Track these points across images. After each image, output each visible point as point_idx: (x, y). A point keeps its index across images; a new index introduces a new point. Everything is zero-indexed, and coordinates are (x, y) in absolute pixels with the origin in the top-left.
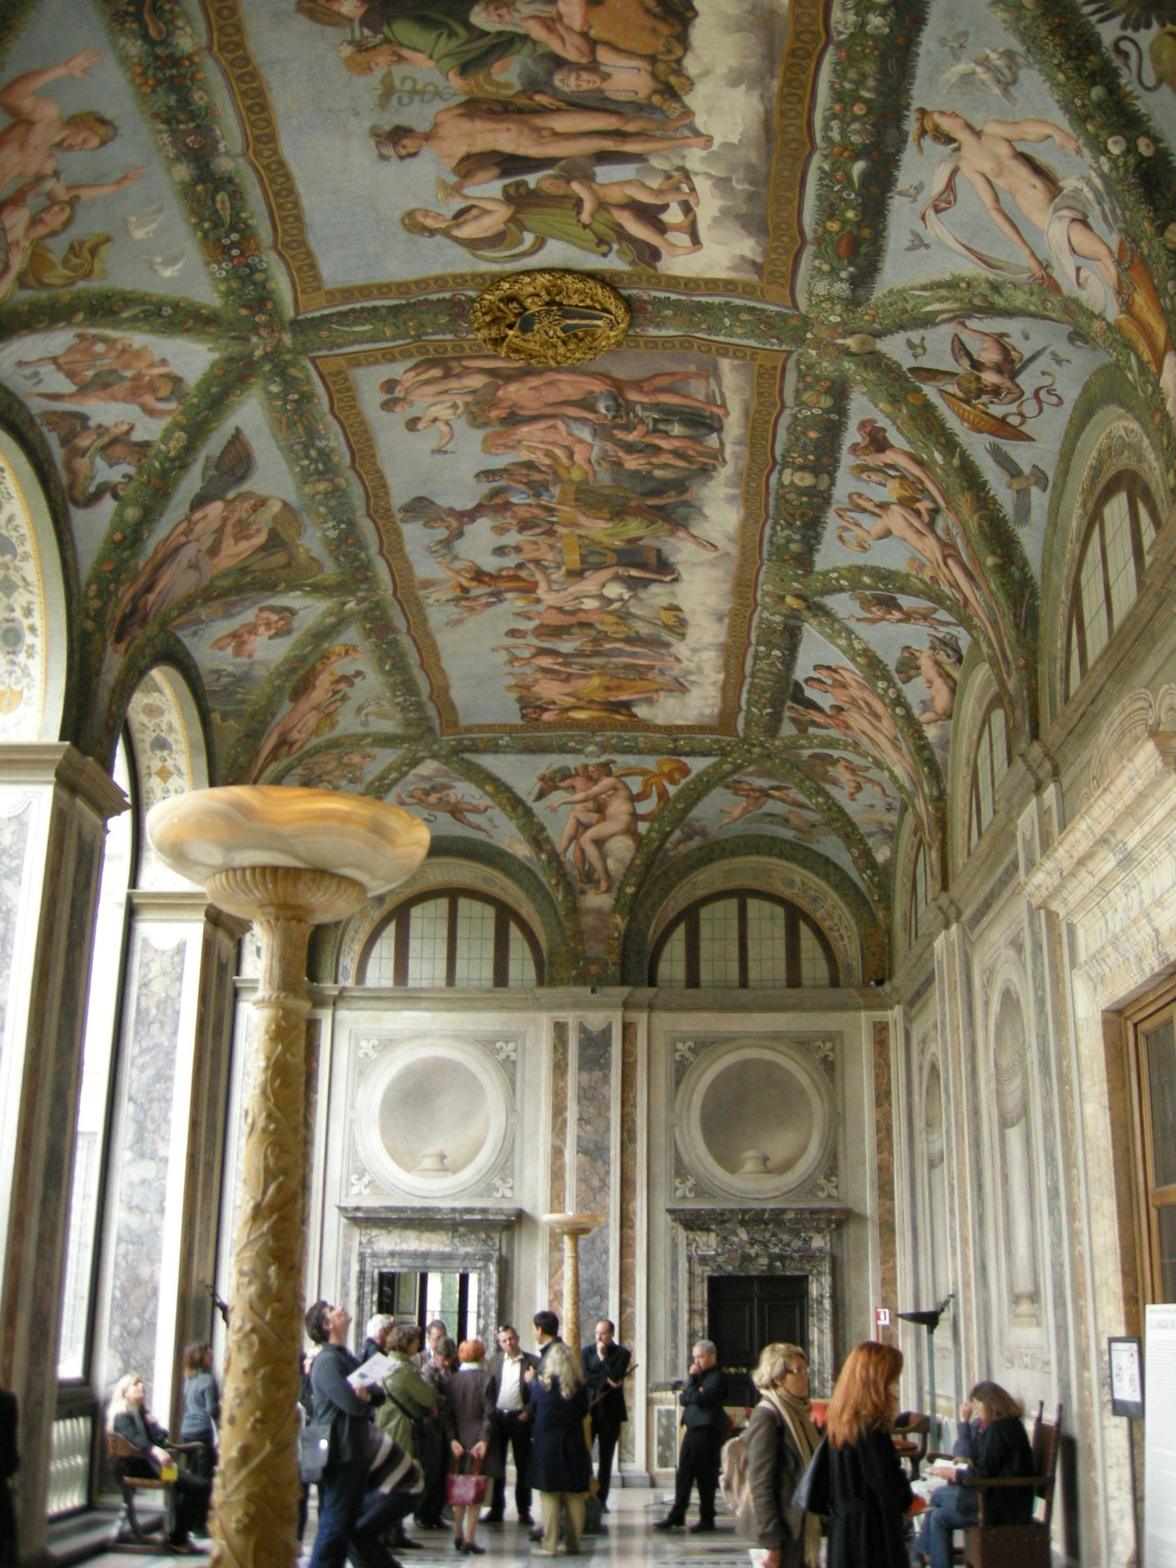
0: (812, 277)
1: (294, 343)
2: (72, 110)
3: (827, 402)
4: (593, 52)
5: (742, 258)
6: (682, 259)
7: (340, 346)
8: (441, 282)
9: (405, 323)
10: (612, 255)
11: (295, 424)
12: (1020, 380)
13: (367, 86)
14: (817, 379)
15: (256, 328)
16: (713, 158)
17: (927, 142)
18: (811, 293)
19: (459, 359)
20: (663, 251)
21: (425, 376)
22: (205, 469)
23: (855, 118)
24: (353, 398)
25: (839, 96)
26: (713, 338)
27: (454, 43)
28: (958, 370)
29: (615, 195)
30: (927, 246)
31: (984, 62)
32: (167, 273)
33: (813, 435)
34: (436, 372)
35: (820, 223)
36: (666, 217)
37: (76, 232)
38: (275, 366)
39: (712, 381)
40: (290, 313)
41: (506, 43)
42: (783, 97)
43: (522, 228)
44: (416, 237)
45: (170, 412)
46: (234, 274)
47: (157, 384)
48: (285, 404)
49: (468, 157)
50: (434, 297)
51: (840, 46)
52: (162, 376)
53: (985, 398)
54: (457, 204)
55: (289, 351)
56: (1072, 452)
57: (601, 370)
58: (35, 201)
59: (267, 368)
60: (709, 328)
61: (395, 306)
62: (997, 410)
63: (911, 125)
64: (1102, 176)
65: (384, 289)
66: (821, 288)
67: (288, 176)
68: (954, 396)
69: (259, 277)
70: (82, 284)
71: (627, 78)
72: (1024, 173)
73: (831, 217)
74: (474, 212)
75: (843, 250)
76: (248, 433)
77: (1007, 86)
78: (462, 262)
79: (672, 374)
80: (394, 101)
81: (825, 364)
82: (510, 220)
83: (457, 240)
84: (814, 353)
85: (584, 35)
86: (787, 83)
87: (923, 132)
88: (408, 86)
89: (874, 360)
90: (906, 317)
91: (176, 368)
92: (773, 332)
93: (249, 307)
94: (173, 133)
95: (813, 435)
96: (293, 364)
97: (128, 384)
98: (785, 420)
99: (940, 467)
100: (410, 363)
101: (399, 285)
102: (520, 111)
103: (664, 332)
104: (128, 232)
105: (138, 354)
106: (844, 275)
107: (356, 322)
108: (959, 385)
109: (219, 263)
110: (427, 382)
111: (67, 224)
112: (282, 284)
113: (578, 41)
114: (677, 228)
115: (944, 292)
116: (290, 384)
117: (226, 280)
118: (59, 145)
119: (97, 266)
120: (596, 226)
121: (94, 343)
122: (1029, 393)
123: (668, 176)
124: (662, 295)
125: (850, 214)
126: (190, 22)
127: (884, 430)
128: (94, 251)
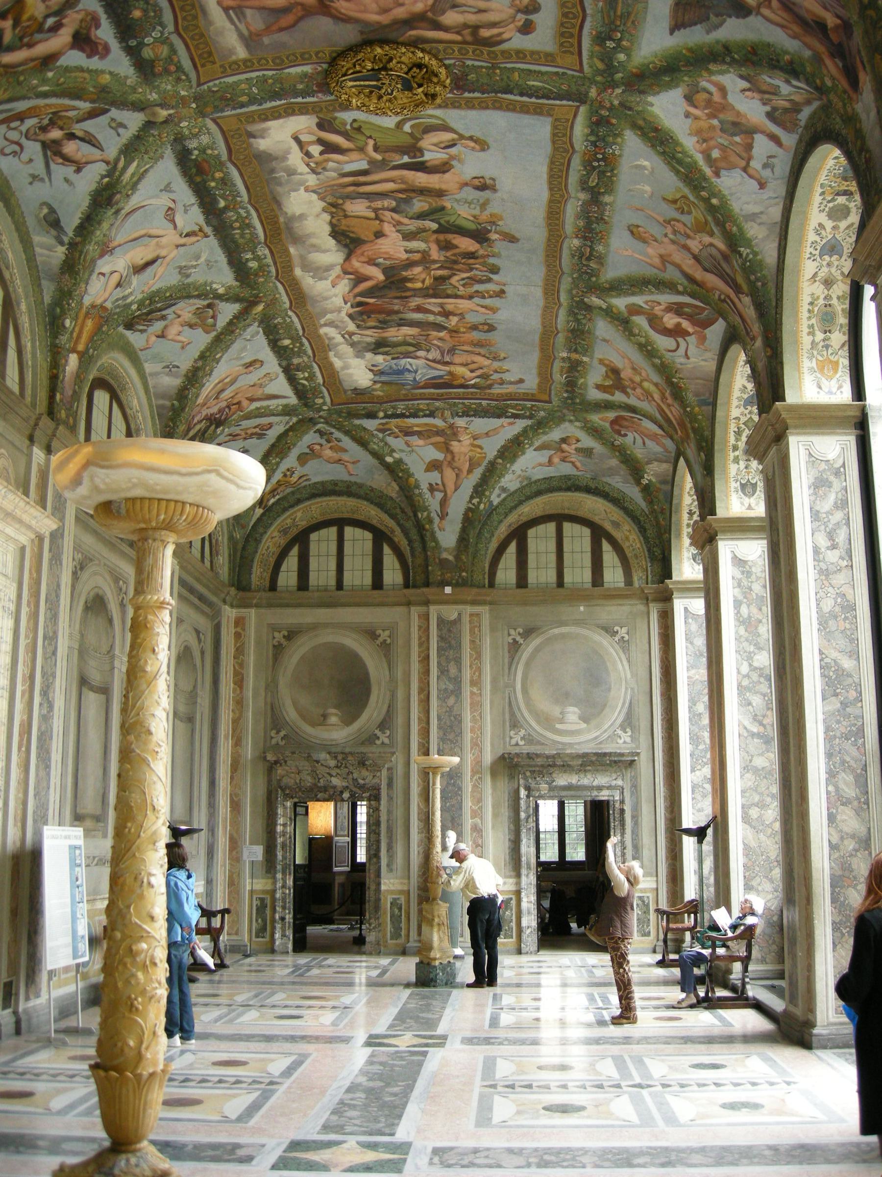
0: (214, 143)
1: (590, 87)
2: (642, 244)
3: (147, 53)
4: (377, 215)
5: (263, 138)
6: (302, 127)
7: (557, 73)
8: (470, 105)
9: (502, 79)
10: (349, 121)
11: (621, 17)
12: (38, 146)
13: (494, 208)
14: (167, 71)
15: (611, 108)
16: (302, 183)
17: (196, 228)
18: (209, 133)
19: (465, 42)
20: (316, 129)
21: (495, 31)
22: (717, 27)
23: (236, 221)
24: (562, 25)
25: (249, 226)
26: (260, 73)
27: (447, 218)
28: (78, 126)
29: (354, 155)
30: (161, 191)
31: (195, 267)
32: (646, 163)
33: (137, 14)
34: (485, 33)
35: (227, 174)
36: (320, 148)
37: (677, 215)
38: (612, 75)
39: (246, 32)
40: (583, 109)
41: (421, 216)
42: (276, 216)
43: (411, 135)
44: (482, 138)
45: (708, 81)
46: (608, 145)
47: (703, 104)
48: (621, 40)
49: (444, 172)
50: (477, 95)
51: (260, 243)
52: (696, 107)
53: (46, 122)
54: (453, 151)
55: (596, 83)
56: (18, 230)
57: (341, 25)
58: (682, 240)
59: (619, 76)
60: (266, 81)
61: (506, 93)
62: (30, 123)
63: (208, 230)
64: (131, 304)
65: (511, 107)
66: (205, 139)
67: (550, 183)
68: (67, 111)
69: (593, 138)
70: (692, 198)
71: (358, 208)
72: (149, 257)
73: (222, 179)
74: (442, 145)
75: (205, 165)
76: (666, 24)
77: (181, 268)
78: (453, 117)
79: (281, 30)
80: (481, 201)
81: (169, 87)
82: (420, 139)
83: (455, 132)
84: (183, 93)
85: (382, 221)
86: (277, 222)
87: (201, 230)
88: (473, 206)
89: (139, 107)
90: (143, 149)
91: (684, 106)
92: (219, 95)
93: (608, 122)
94: (602, 214)
95: (137, 14)
96: (598, 72)
97: (721, 116)
98: (168, 16)
99: (37, 86)
100: (505, 46)
101: (500, 108)
102: (414, 191)
103: (298, 70)
104: (652, 193)
105: (698, 132)
106: (196, 152)
107: (538, 89)
108: (69, 118)
109: (613, 154)
110: (494, 25)
111: (675, 220)
112: (580, 129)
113: (385, 219)
114: (311, 143)
115: (135, 179)
116: (607, 58)
117: (615, 144)
118: (656, 240)
119: (678, 196)
120: (364, 138)
121: (716, 160)
122: (24, 141)
123: (324, 169)
124: (309, 99)
125: (213, 184)
126: (570, 248)
127: (89, 56)
128: (675, 202)
